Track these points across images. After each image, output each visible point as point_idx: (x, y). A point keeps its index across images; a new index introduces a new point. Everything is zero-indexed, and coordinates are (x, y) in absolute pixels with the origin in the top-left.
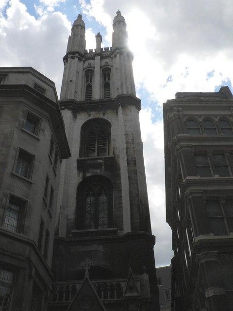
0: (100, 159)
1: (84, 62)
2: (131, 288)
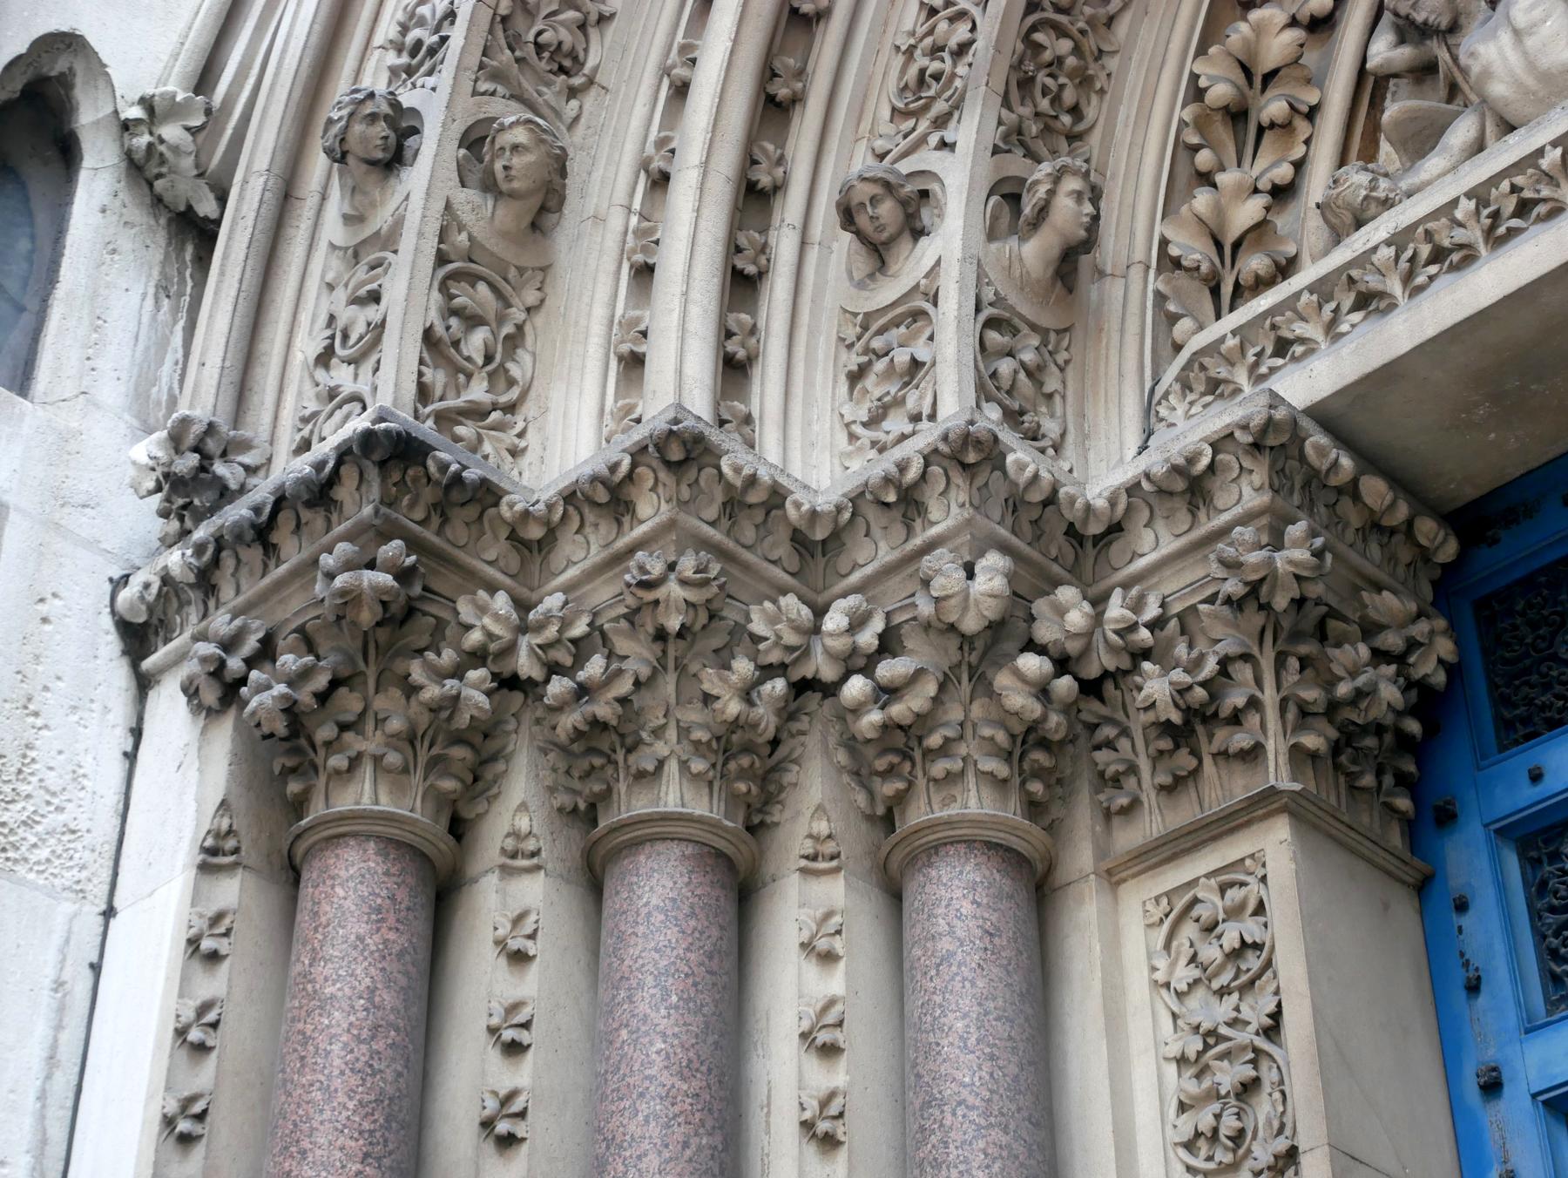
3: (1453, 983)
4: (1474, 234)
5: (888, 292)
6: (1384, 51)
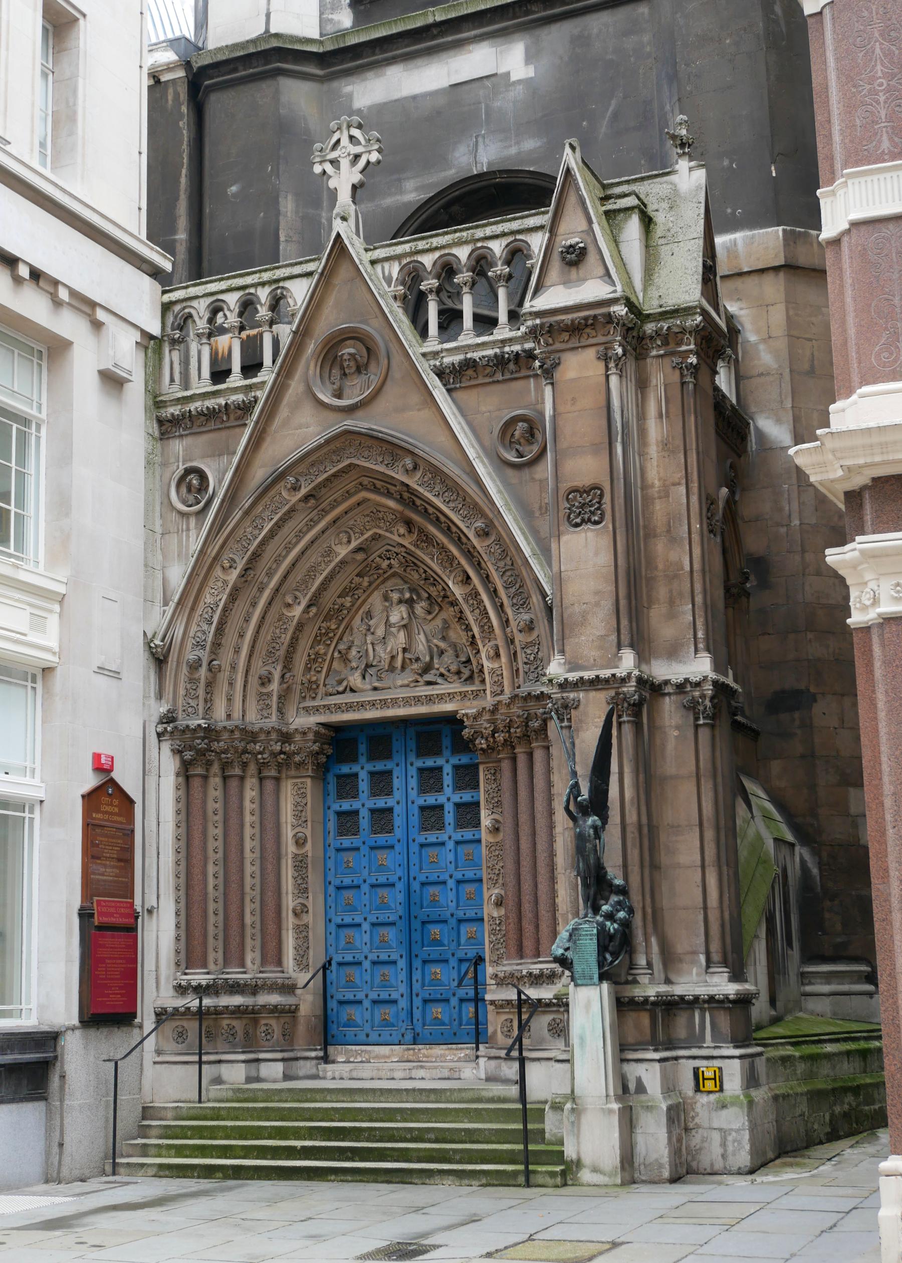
2: (575, 257)
3: (326, 794)
4: (344, 709)
5: (264, 690)
6: (336, 654)
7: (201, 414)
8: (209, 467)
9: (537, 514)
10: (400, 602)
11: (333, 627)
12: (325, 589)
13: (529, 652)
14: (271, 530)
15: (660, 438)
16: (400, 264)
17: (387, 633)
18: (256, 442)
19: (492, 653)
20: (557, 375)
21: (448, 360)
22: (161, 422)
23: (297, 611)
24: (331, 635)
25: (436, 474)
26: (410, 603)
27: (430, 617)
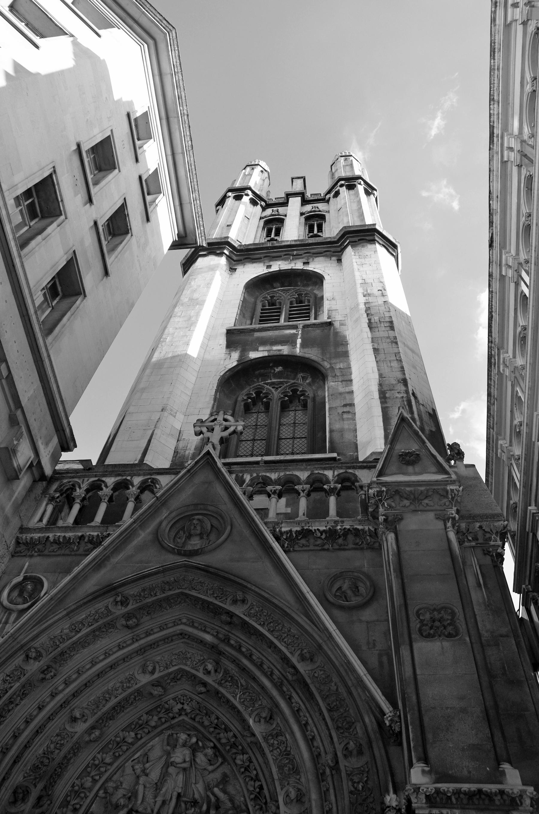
0: (295, 327)
1: (264, 209)
6: (101, 792)
7: (56, 542)
8: (47, 579)
9: (364, 648)
10: (184, 745)
11: (108, 760)
12: (112, 718)
13: (356, 779)
14: (87, 635)
15: (481, 601)
16: (251, 476)
17: (164, 775)
18: (98, 565)
19: (293, 795)
20: (401, 527)
21: (285, 529)
22: (18, 543)
23: (81, 727)
24: (103, 769)
25: (267, 602)
26: (194, 749)
27: (210, 768)
